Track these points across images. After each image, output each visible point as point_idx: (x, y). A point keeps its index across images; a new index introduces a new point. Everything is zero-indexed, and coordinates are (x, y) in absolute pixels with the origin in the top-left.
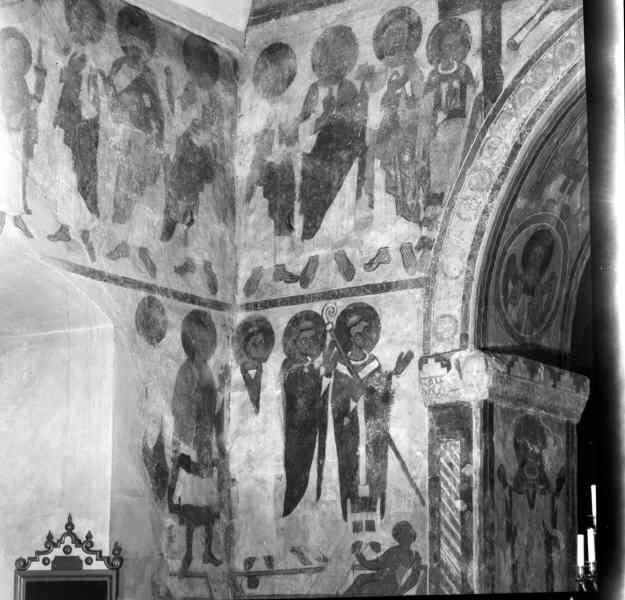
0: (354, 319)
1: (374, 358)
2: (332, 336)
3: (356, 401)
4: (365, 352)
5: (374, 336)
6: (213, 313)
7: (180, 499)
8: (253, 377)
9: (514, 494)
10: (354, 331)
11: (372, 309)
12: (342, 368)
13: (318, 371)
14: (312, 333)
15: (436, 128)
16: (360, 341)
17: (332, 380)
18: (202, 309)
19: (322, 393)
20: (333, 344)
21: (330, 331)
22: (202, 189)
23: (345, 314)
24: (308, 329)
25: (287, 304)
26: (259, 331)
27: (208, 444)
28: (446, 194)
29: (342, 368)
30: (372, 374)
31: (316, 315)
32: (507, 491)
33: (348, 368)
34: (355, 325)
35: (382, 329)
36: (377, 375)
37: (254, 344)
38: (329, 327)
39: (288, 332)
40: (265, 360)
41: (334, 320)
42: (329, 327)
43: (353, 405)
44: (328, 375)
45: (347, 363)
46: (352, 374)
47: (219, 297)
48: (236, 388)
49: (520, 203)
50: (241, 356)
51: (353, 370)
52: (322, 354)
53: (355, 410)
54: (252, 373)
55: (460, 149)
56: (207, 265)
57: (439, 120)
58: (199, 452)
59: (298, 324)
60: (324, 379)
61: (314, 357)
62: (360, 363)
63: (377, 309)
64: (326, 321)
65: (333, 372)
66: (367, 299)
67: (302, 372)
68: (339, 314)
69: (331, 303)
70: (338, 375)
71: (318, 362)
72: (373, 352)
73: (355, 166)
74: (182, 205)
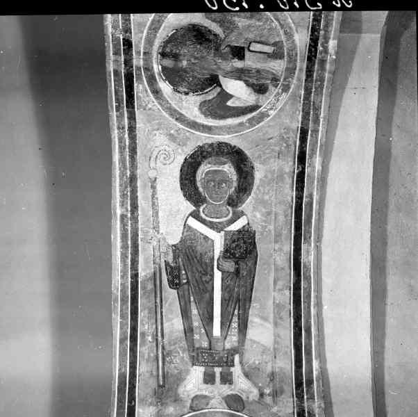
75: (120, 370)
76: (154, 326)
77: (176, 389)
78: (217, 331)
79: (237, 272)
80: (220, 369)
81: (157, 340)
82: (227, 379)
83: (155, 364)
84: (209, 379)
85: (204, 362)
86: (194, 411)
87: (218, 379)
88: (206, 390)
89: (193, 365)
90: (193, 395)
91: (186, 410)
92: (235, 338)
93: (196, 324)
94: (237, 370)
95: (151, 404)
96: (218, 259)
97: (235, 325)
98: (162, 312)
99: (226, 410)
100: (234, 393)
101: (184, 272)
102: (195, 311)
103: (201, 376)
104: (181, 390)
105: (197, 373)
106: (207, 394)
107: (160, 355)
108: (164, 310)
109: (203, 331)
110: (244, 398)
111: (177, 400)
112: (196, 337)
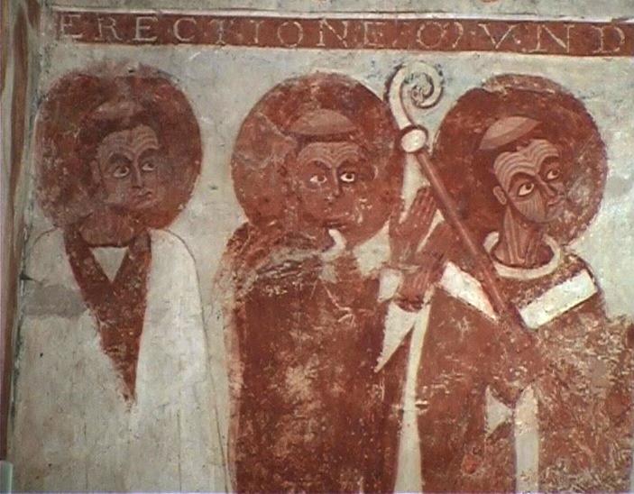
0: (502, 129)
1: (579, 266)
2: (423, 171)
3: (509, 399)
4: (550, 241)
8: (111, 275)
10: (506, 166)
11: (575, 105)
12: (459, 283)
13: (374, 283)
14: (350, 150)
16: (532, 205)
17: (421, 319)
19: (382, 361)
20: (428, 198)
21: (417, 153)
23: (479, 104)
24: (333, 137)
25: (249, 42)
26: (140, 118)
29: (459, 283)
30: (566, 321)
31: (362, 94)
33: (486, 291)
34: (511, 147)
35: (610, 174)
36: (590, 324)
37: (124, 163)
38: (413, 142)
39: (252, 137)
40: (165, 217)
41: (434, 119)
42: (413, 142)
43: (496, 413)
44: (410, 301)
45: (477, 266)
46: (496, 310)
48: (48, 302)
50: (66, 196)
51: (509, 297)
52: (386, 228)
53: (505, 430)
54: (110, 259)
59: (293, 113)
60: (394, 309)
61: (356, 234)
62: (534, 274)
63: (591, 106)
64: (403, 123)
65: (428, 295)
66: (560, 70)
67: (310, 277)
68: (448, 103)
69: (421, 63)
70: (445, 305)
71: (373, 254)
72: (576, 246)
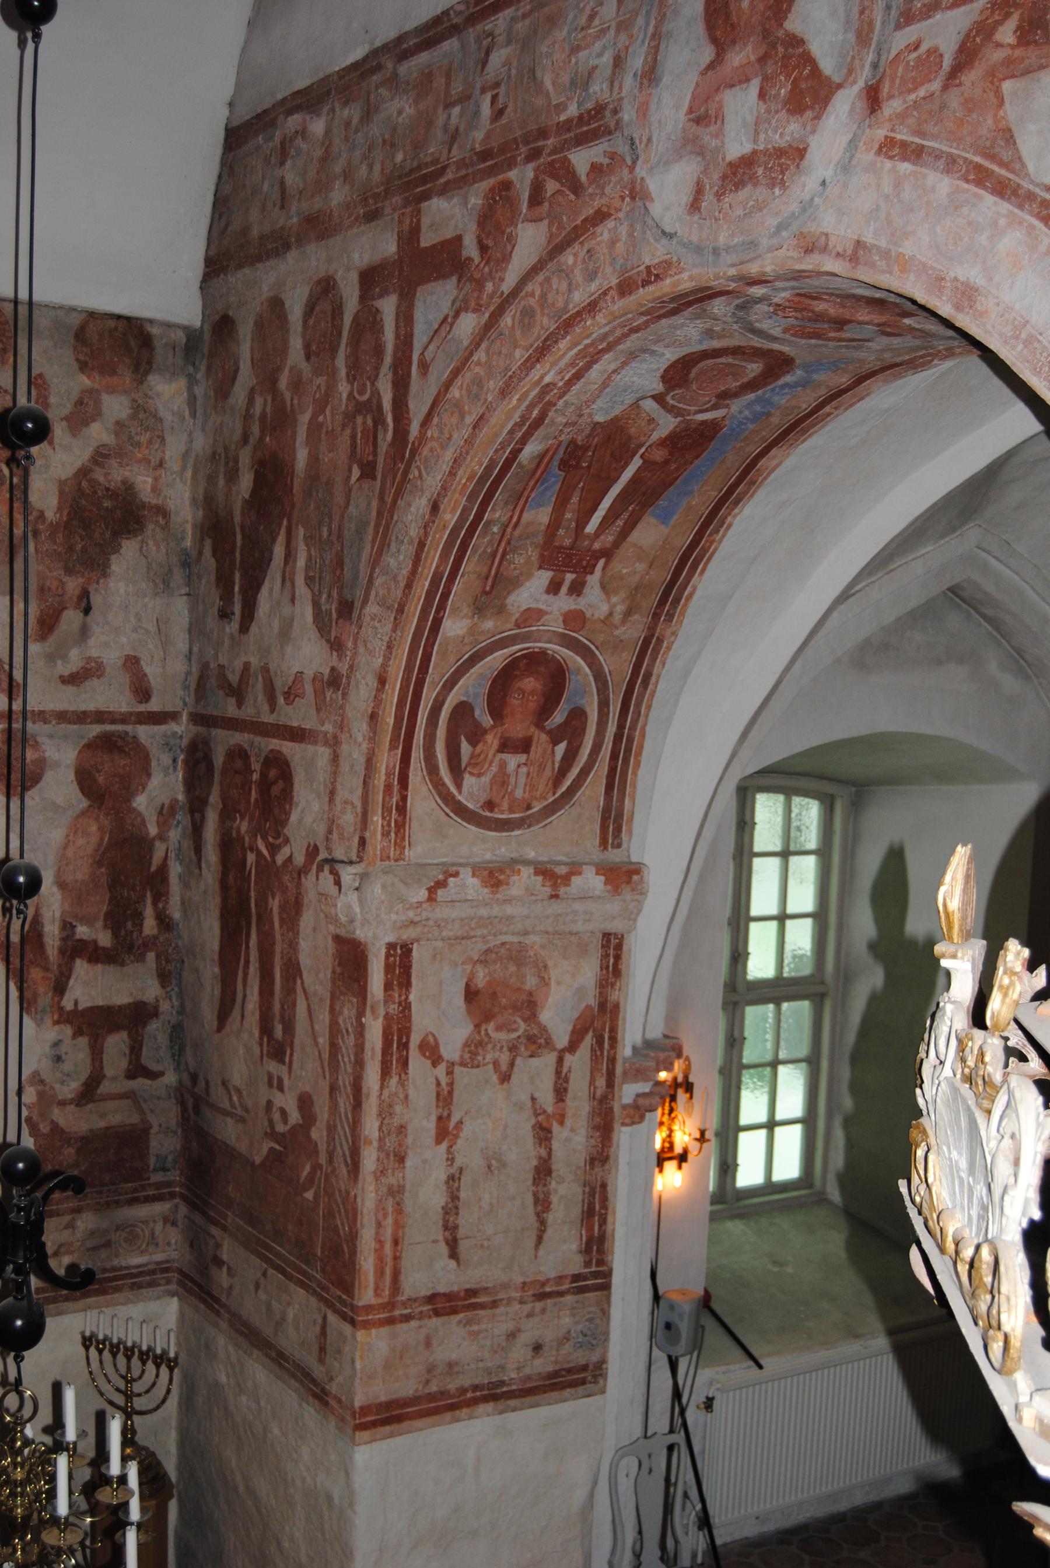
5: (287, 807)
6: (144, 733)
7: (76, 1003)
9: (458, 1069)
15: (350, 490)
18: (119, 727)
22: (117, 549)
27: (138, 918)
28: (356, 603)
32: (441, 1070)
47: (154, 705)
49: (453, 627)
55: (370, 530)
56: (132, 663)
57: (354, 479)
58: (115, 935)
73: (281, 538)
74: (73, 585)
75: (437, 567)
76: (509, 514)
77: (505, 598)
78: (591, 528)
79: (666, 462)
80: (573, 576)
81: (505, 531)
82: (577, 589)
83: (489, 562)
84: (554, 588)
85: (557, 565)
86: (519, 628)
87: (564, 589)
88: (545, 602)
89: (540, 568)
90: (524, 607)
91: (511, 626)
92: (611, 538)
93: (568, 516)
94: (593, 580)
95: (465, 616)
96: (650, 446)
97: (620, 522)
98: (528, 497)
99: (560, 630)
100: (579, 607)
101: (590, 453)
102: (575, 499)
103: (547, 582)
104: (510, 600)
105: (544, 577)
106: (544, 607)
107: (501, 550)
108: (533, 495)
109: (573, 524)
110: (588, 615)
111: (502, 610)
112: (561, 532)
